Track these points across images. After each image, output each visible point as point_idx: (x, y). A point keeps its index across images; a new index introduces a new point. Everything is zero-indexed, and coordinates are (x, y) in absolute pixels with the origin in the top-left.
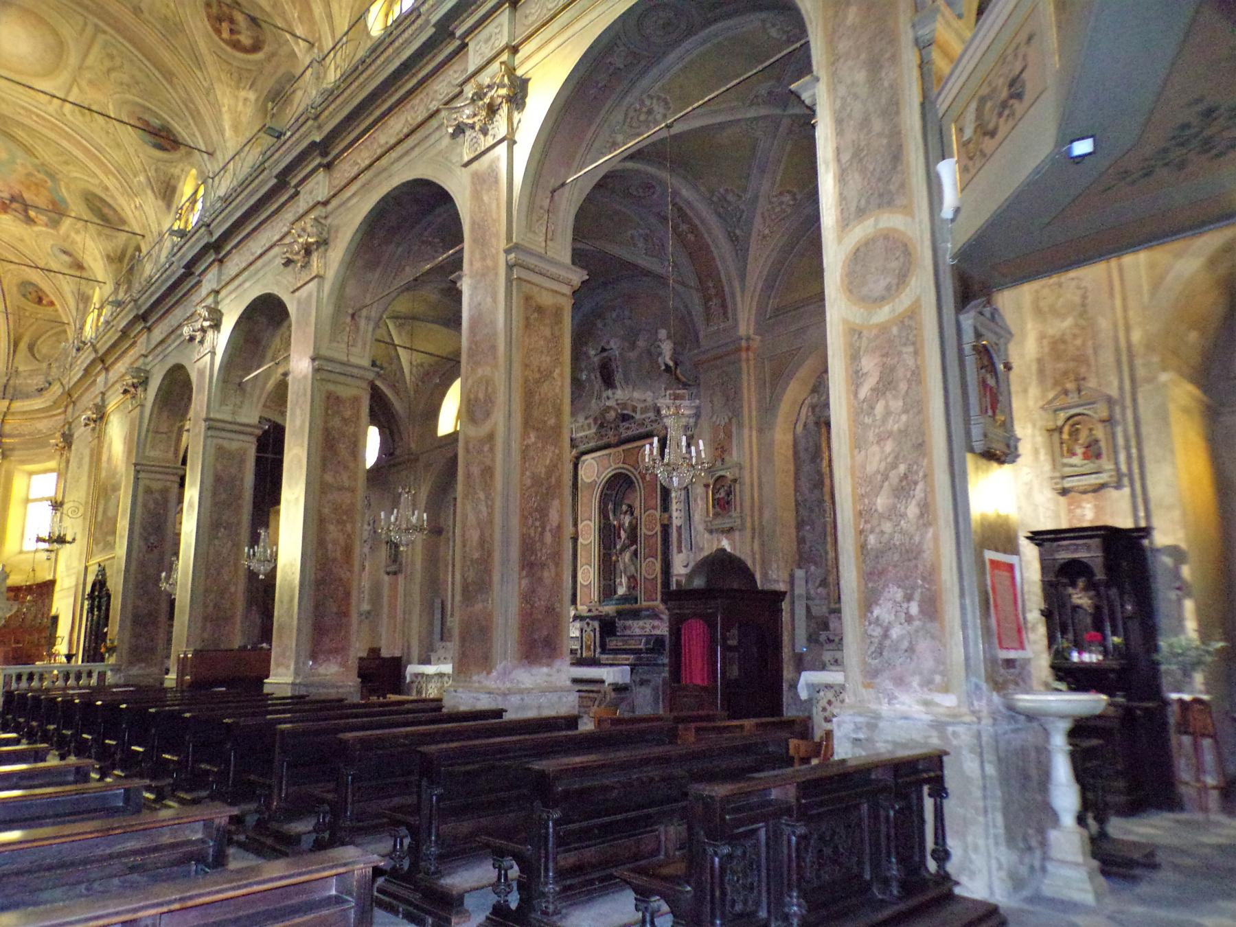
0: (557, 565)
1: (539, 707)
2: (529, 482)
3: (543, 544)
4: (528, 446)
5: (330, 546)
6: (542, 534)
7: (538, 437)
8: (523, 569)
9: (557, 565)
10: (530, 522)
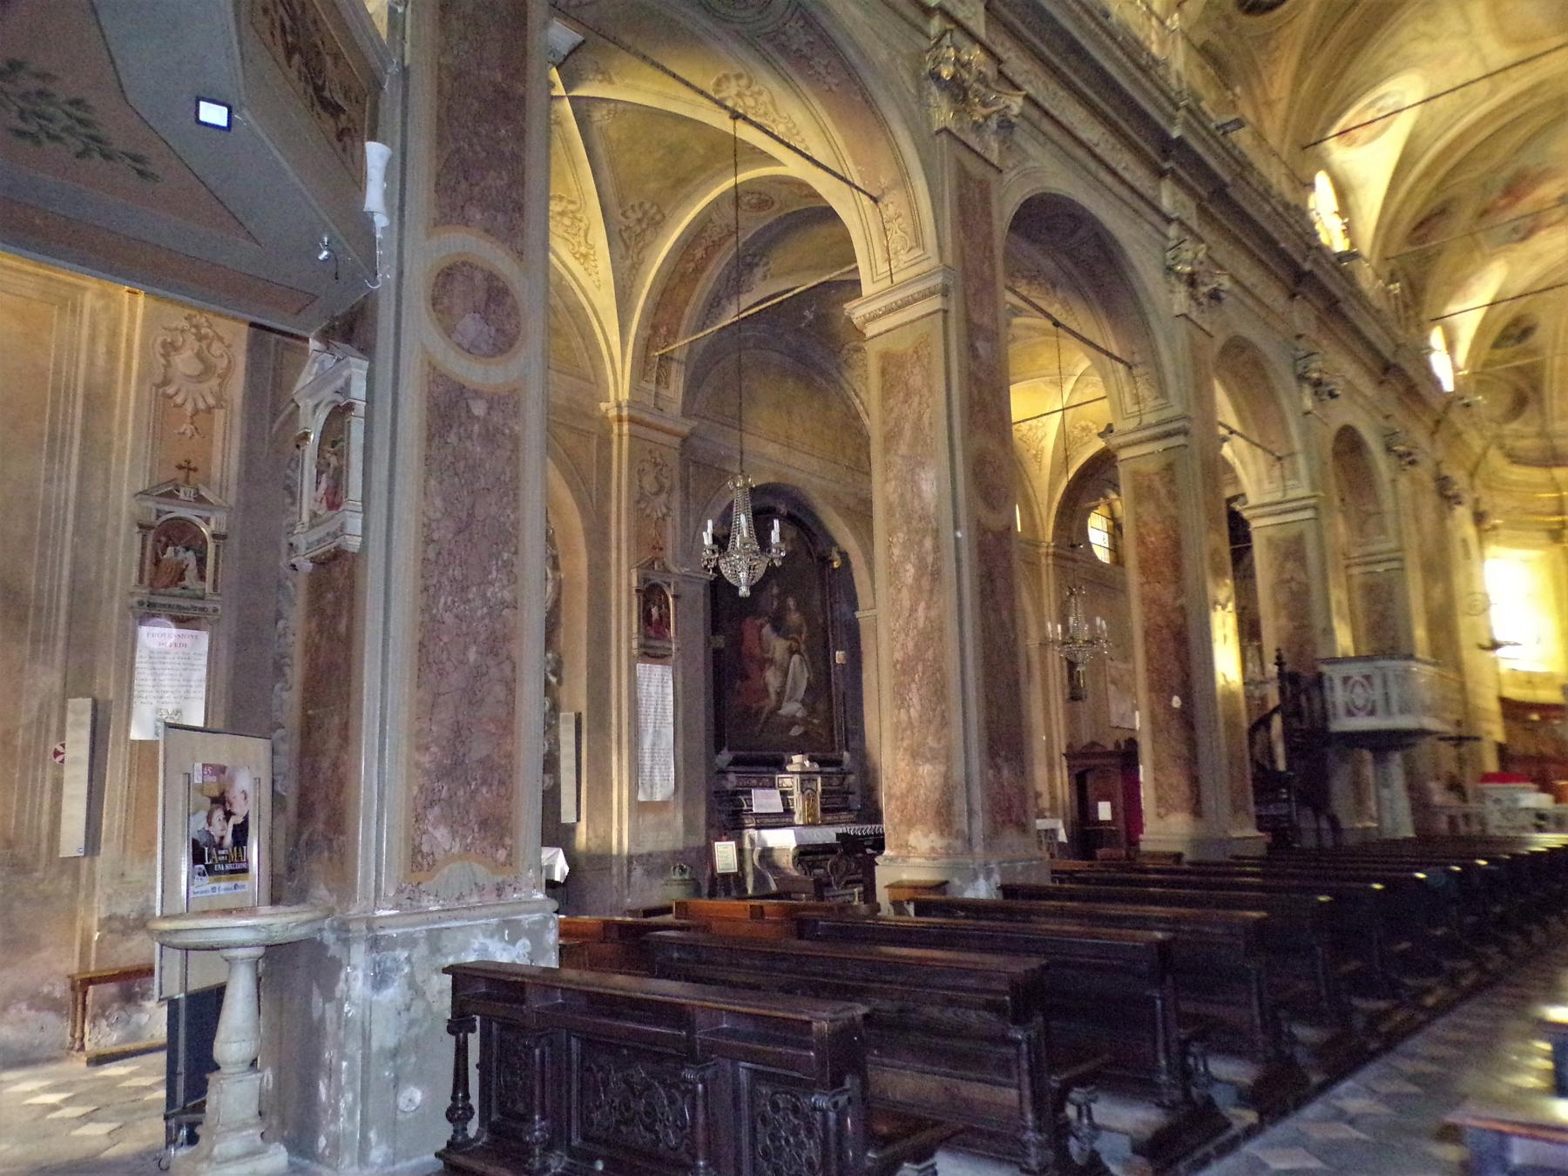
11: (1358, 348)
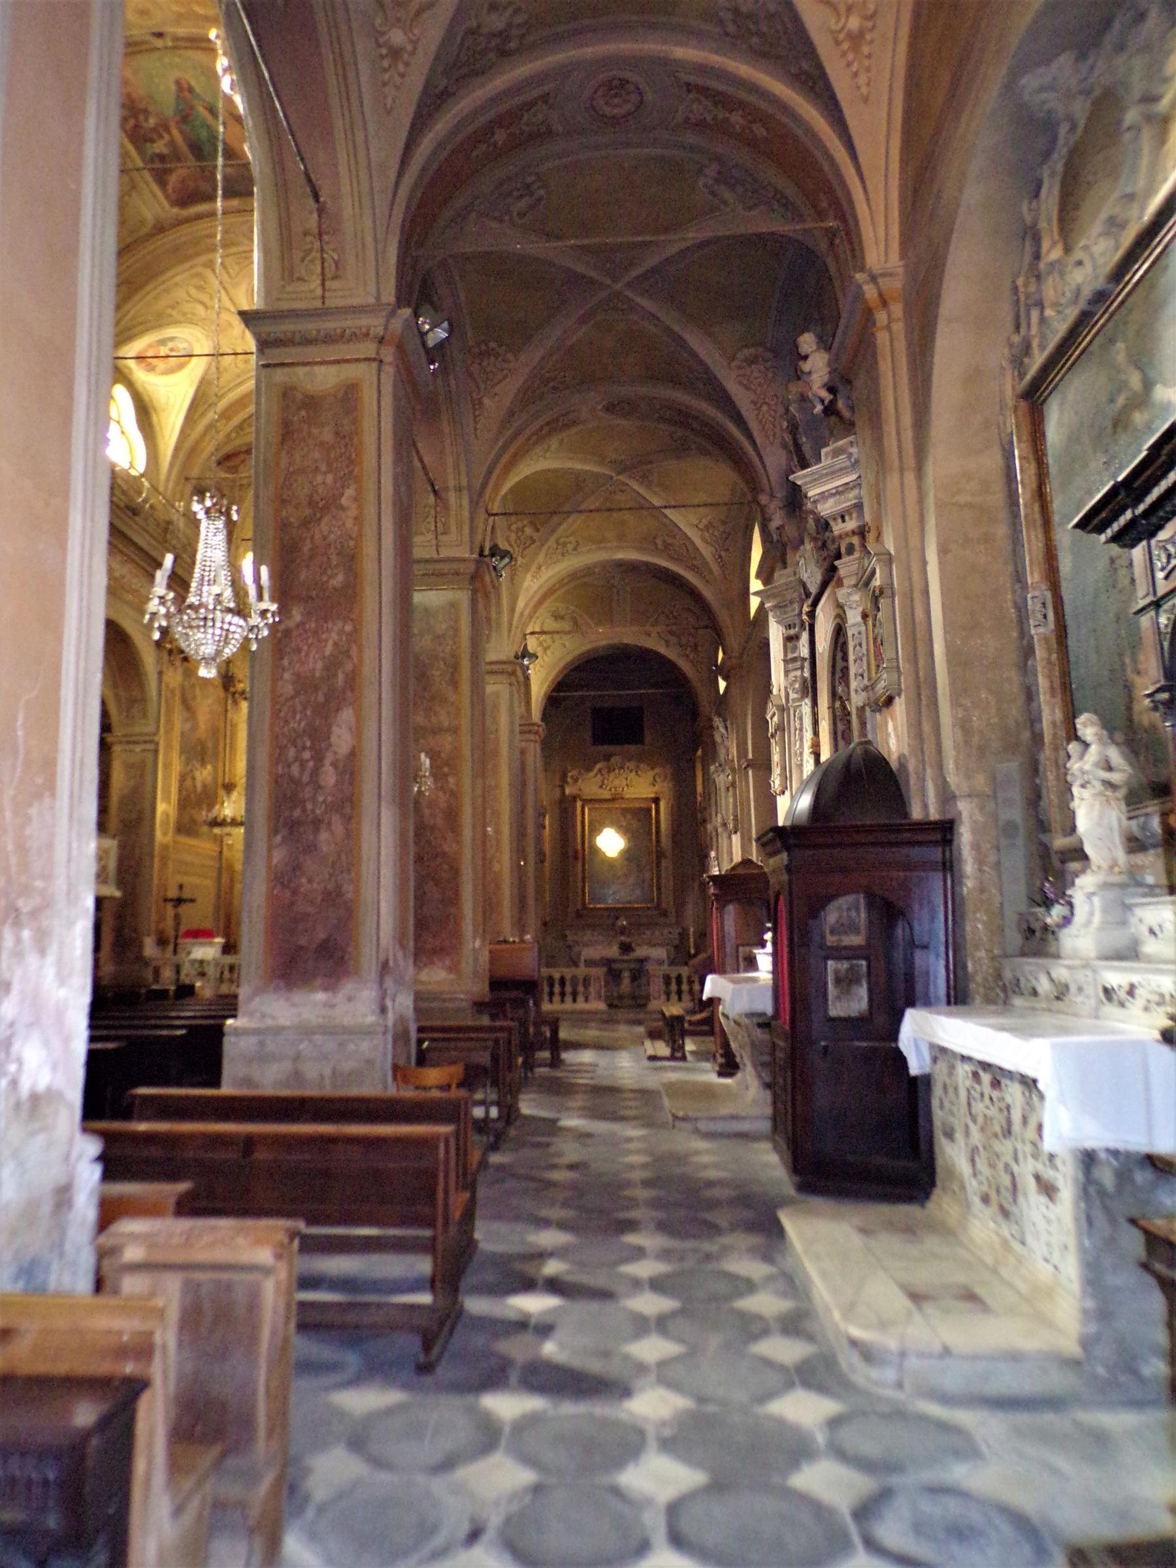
0: (348, 819)
1: (297, 1058)
2: (289, 689)
3: (318, 787)
5: (427, 812)
6: (316, 772)
7: (308, 614)
9: (348, 819)
10: (292, 752)
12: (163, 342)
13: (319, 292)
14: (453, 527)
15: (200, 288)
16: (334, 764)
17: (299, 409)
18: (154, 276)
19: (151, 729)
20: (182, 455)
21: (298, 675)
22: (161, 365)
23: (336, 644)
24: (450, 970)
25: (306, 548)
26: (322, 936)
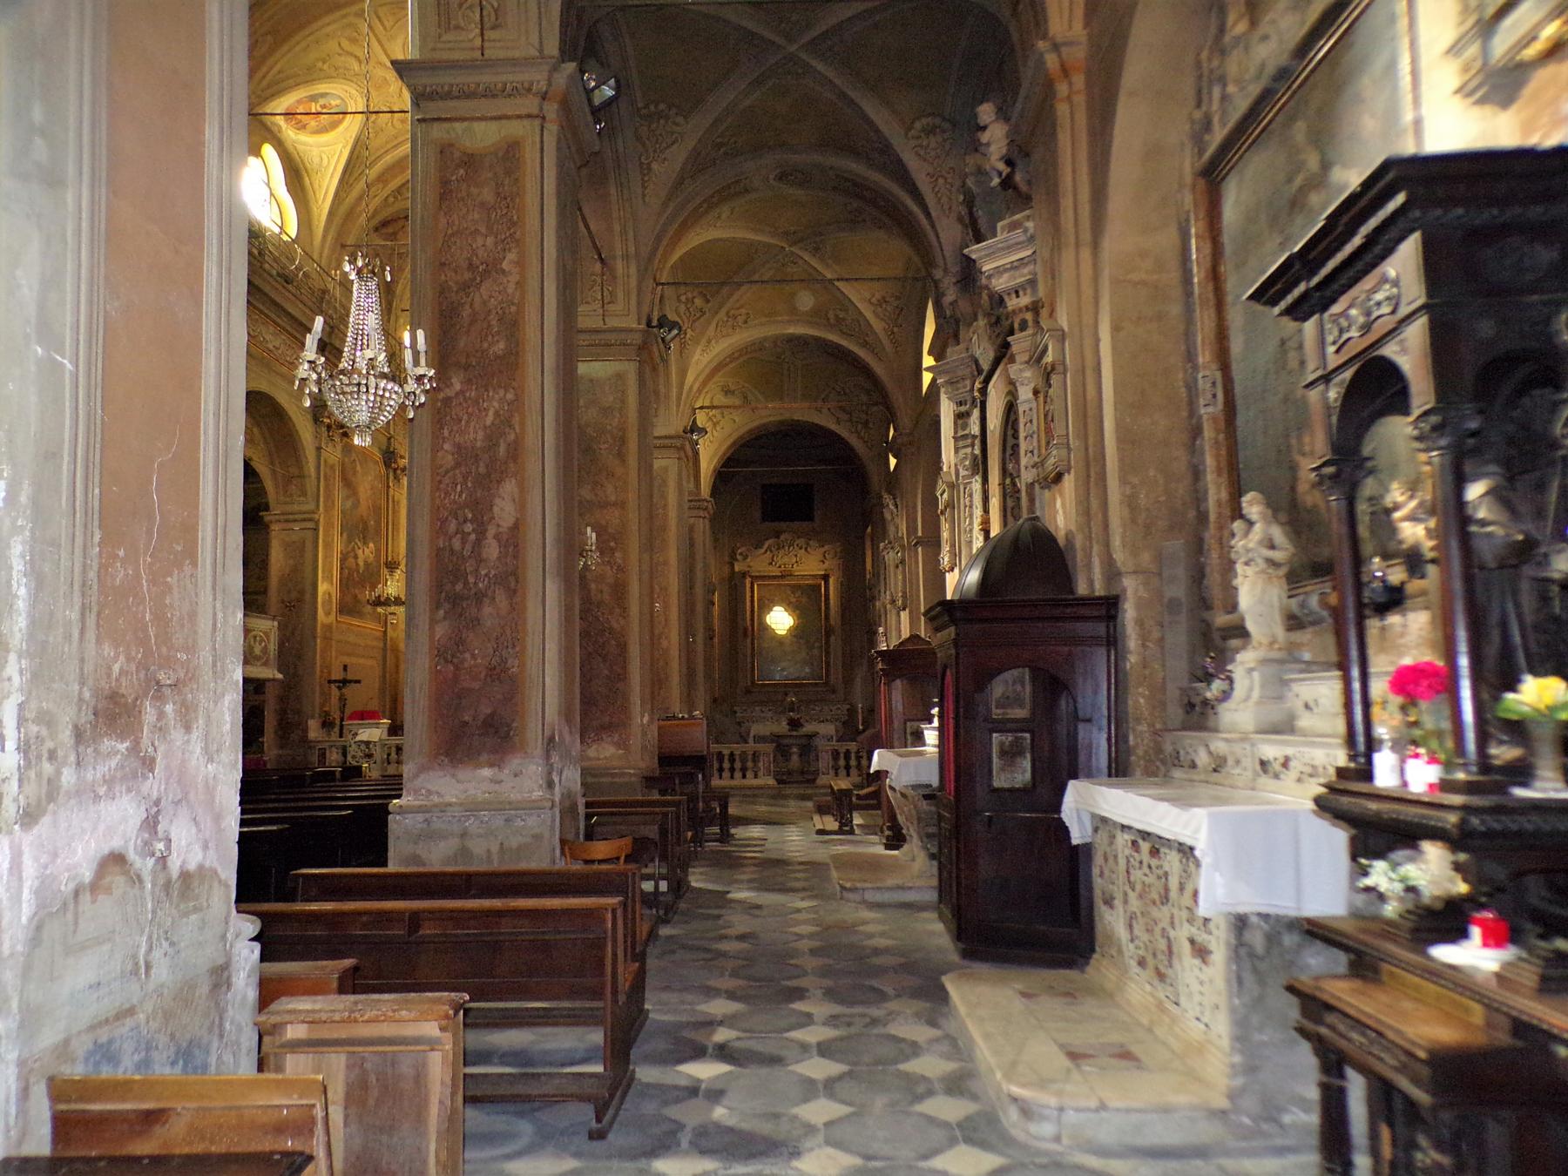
0: (512, 593)
1: (464, 835)
3: (481, 561)
4: (447, 401)
6: (479, 543)
8: (438, 606)
9: (512, 593)
11: (283, 321)
12: (313, 98)
13: (478, 42)
14: (620, 295)
15: (353, 41)
16: (497, 537)
17: (458, 166)
18: (302, 27)
19: (311, 506)
20: (338, 220)
21: (458, 447)
22: (313, 123)
23: (497, 414)
24: (618, 745)
25: (466, 312)
26: (486, 710)
